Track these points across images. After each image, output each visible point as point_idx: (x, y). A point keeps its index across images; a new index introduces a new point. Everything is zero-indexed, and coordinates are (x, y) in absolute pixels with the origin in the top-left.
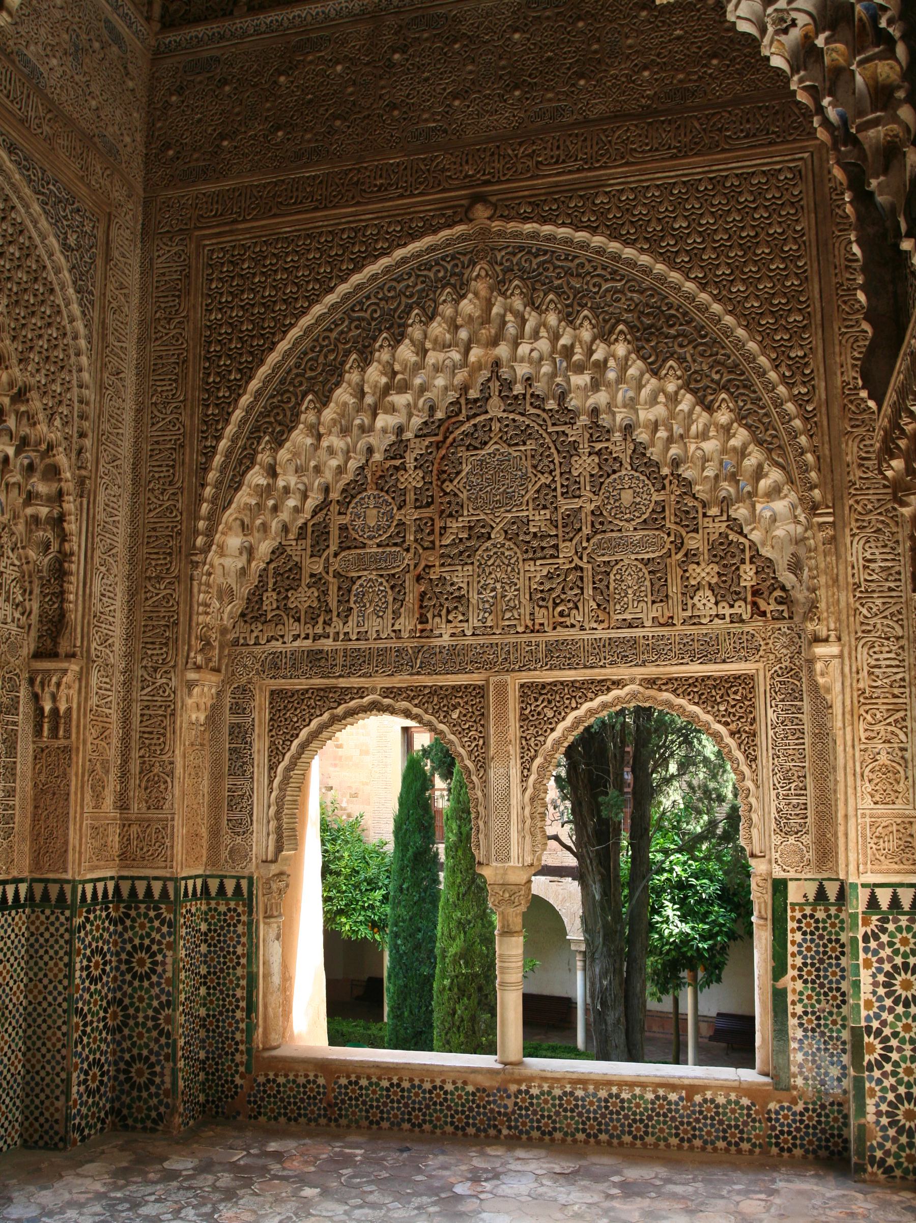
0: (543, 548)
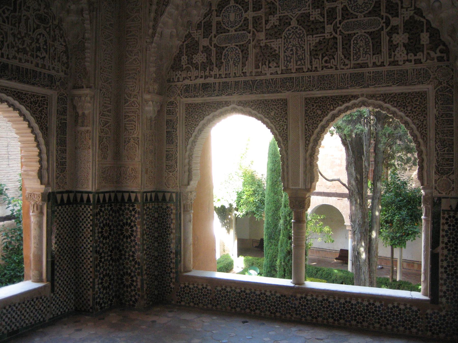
0: (317, 29)
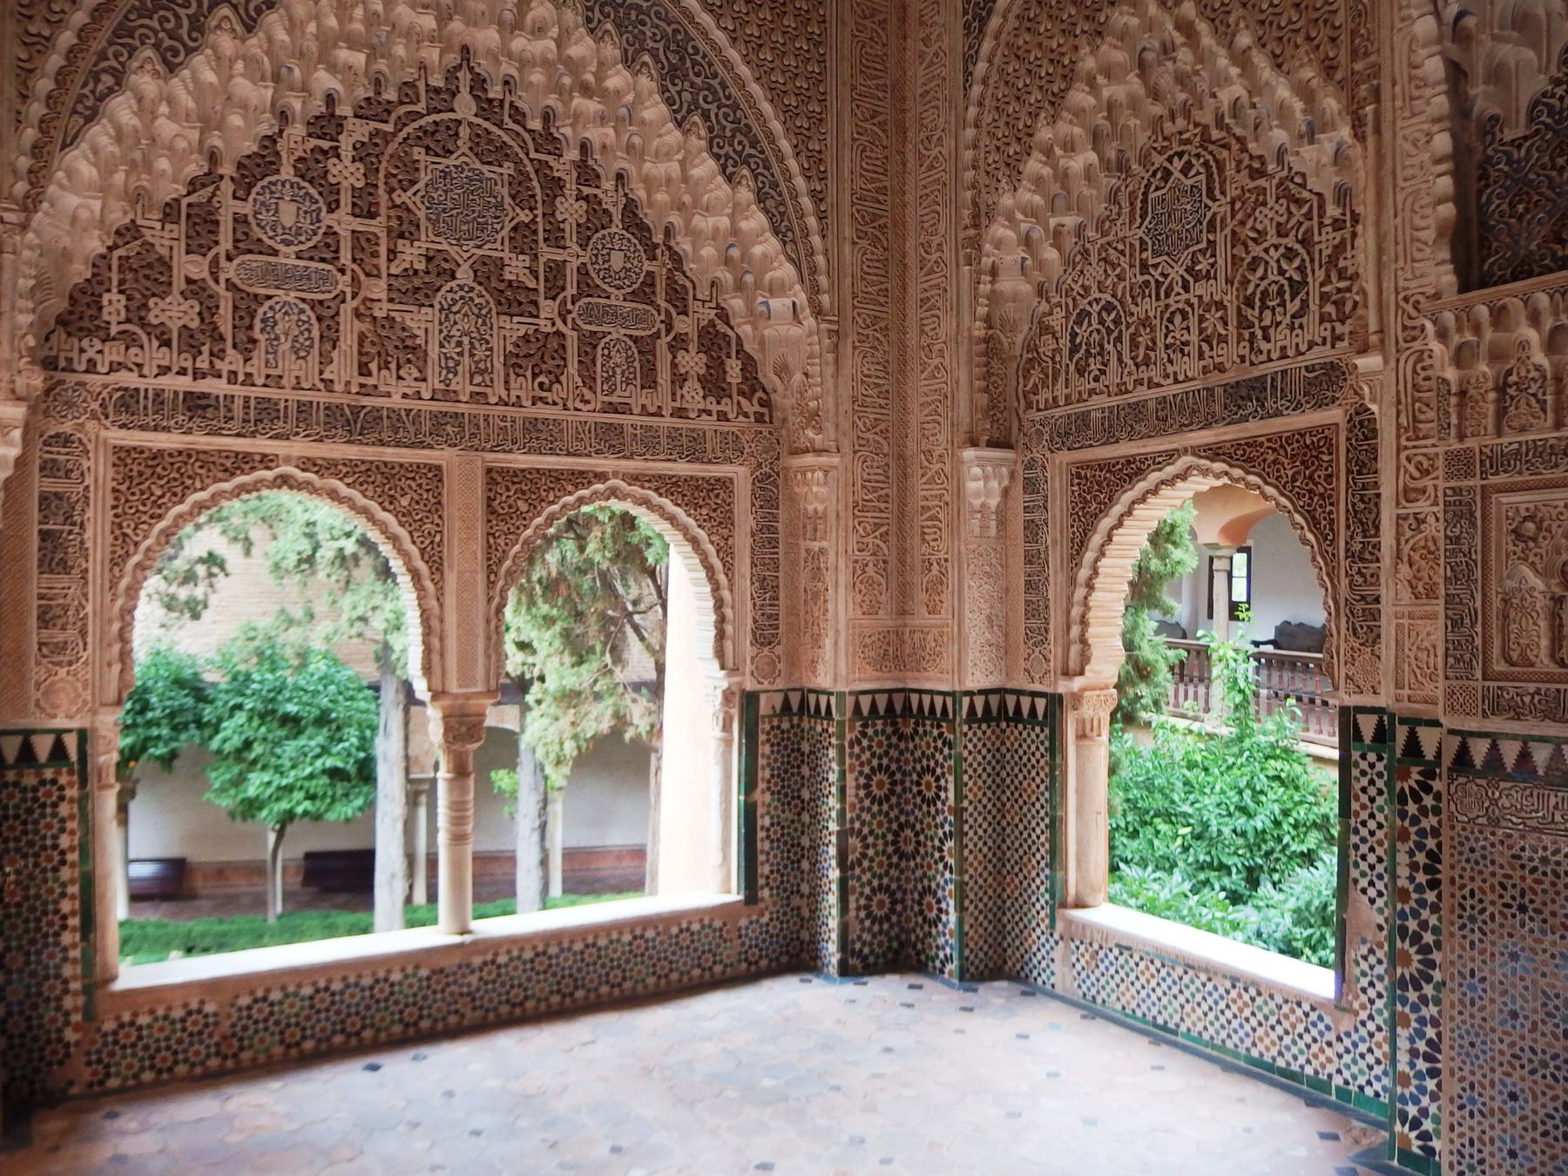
0: (520, 303)
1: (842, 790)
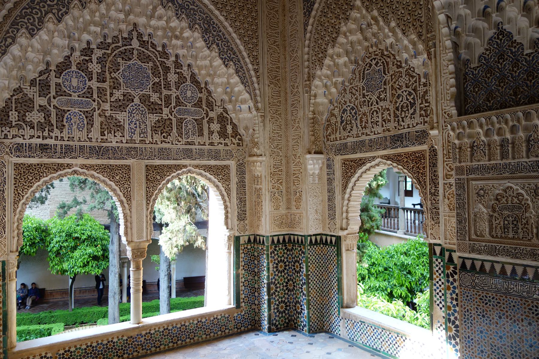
0: (156, 109)
1: (268, 269)
